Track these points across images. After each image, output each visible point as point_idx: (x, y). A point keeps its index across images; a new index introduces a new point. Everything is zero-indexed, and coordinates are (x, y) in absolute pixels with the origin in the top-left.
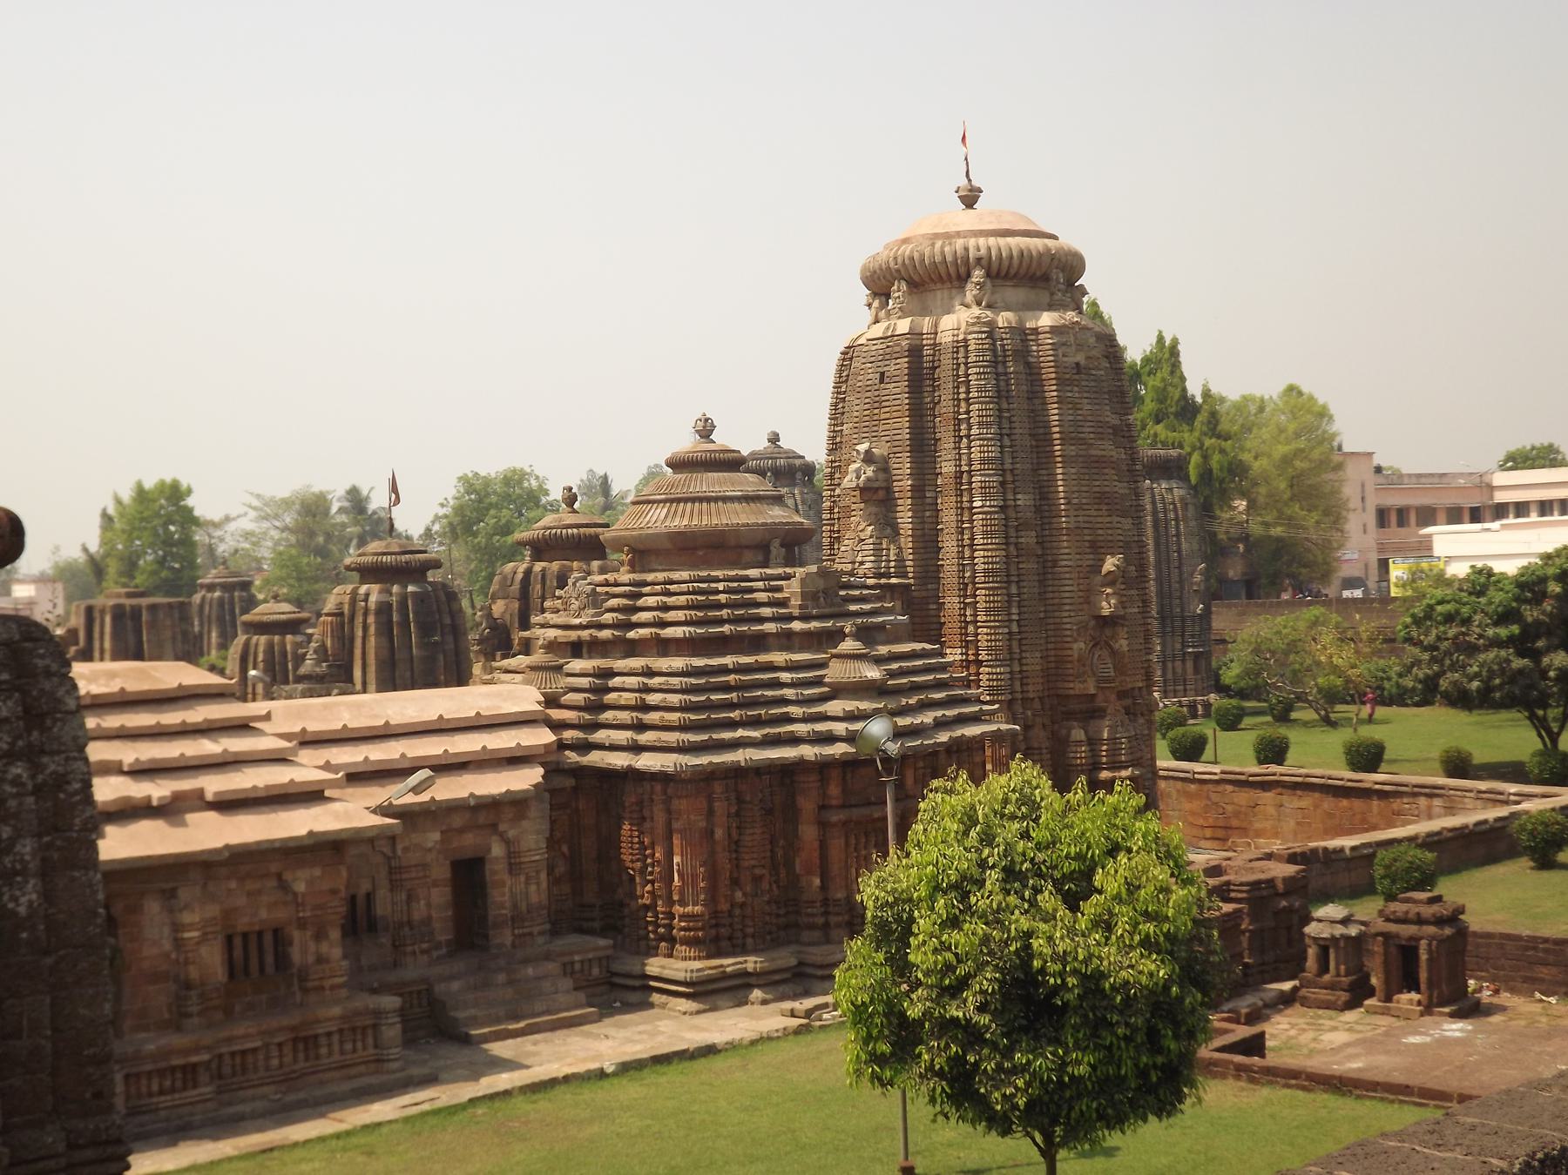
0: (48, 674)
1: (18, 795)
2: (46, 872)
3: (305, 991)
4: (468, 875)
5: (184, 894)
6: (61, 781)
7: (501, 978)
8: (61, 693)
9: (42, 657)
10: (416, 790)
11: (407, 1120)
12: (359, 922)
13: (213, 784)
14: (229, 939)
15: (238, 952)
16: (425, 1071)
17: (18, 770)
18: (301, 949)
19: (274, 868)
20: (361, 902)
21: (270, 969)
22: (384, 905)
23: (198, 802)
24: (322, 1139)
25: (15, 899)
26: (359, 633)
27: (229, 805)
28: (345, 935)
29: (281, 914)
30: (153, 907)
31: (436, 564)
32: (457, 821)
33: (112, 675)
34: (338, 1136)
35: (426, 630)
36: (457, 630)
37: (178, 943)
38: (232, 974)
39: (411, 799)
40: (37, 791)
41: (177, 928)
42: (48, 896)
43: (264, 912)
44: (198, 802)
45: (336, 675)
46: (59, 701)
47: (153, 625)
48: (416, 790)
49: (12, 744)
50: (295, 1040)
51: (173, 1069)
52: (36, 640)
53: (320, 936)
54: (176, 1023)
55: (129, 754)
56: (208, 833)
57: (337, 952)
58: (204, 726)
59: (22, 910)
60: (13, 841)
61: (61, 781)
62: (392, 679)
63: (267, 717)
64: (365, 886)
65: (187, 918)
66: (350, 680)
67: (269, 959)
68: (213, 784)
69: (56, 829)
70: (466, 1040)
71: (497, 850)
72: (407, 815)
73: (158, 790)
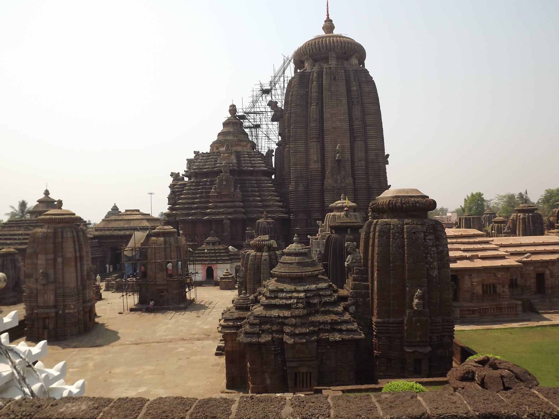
0: (440, 231)
3: (500, 298)
4: (540, 277)
5: (473, 275)
6: (442, 251)
7: (548, 300)
10: (526, 258)
11: (521, 328)
12: (513, 284)
13: (480, 254)
14: (483, 285)
15: (485, 288)
16: (527, 318)
18: (499, 289)
19: (493, 272)
20: (514, 281)
21: (492, 293)
22: (519, 281)
23: (477, 257)
24: (500, 329)
26: (518, 224)
27: (484, 258)
28: (509, 286)
29: (495, 281)
30: (467, 278)
31: (537, 209)
32: (538, 265)
33: (459, 231)
34: (504, 329)
35: (534, 223)
36: (542, 223)
37: (472, 285)
38: (483, 292)
39: (525, 259)
40: (438, 253)
41: (472, 282)
42: (439, 273)
43: (491, 281)
44: (477, 257)
45: (513, 232)
47: (473, 221)
48: (526, 258)
50: (497, 308)
51: (470, 310)
53: (503, 287)
54: (471, 301)
55: (463, 247)
56: (479, 264)
57: (507, 290)
60: (432, 263)
61: (442, 251)
62: (525, 234)
63: (493, 241)
64: (515, 277)
65: (474, 280)
66: (516, 234)
67: (492, 290)
68: (480, 254)
70: (538, 313)
71: (548, 272)
72: (524, 263)
73: (468, 254)
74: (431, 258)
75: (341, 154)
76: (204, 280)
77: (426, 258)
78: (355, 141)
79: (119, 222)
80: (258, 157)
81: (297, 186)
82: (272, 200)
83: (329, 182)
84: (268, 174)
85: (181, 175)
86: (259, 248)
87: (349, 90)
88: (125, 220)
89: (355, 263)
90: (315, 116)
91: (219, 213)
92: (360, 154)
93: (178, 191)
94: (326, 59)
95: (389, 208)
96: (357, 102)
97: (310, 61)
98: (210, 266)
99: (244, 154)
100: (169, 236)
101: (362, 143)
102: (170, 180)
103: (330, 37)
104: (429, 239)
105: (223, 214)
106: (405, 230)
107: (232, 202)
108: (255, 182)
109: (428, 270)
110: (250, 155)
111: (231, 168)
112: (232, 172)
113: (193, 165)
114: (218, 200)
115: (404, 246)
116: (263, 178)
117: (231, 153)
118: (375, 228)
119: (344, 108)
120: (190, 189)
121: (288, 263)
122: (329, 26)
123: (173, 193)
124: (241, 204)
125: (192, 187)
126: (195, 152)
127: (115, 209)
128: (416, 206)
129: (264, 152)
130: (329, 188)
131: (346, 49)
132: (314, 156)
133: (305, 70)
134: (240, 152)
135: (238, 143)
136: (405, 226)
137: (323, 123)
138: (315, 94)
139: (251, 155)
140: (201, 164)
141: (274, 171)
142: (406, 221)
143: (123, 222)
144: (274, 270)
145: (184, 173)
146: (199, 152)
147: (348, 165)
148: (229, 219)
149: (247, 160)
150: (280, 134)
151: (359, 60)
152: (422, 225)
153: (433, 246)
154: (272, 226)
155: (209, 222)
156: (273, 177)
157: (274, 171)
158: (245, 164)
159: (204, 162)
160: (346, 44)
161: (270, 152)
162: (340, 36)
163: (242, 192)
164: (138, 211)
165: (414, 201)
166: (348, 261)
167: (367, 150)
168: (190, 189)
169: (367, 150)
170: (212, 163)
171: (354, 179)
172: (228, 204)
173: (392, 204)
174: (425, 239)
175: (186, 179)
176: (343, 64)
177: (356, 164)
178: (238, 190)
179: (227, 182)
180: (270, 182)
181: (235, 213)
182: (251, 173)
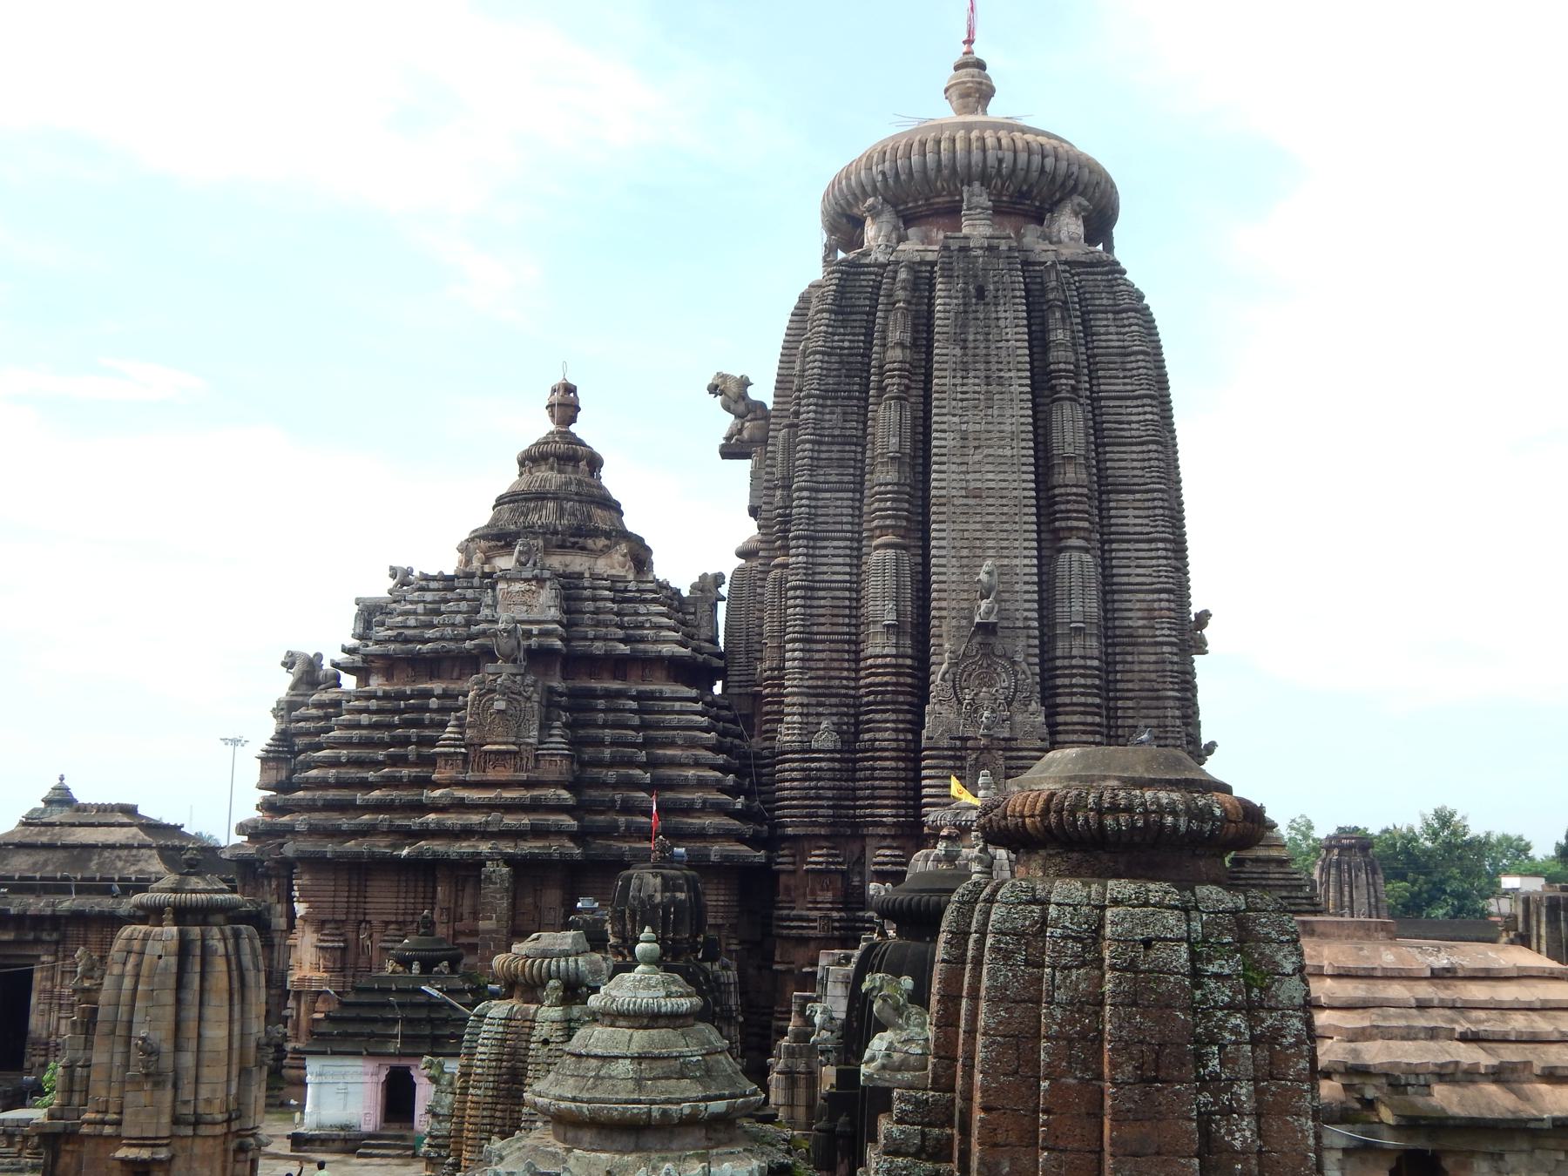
0: (1270, 941)
1: (1236, 1043)
2: (1258, 1115)
8: (1279, 957)
9: (1264, 925)
17: (1237, 1020)
25: (1231, 1133)
40: (1255, 1041)
42: (1260, 1133)
46: (1277, 964)
49: (1232, 999)
52: (1256, 910)
58: (1538, 1005)
59: (1238, 1144)
60: (1231, 1081)
69: (1273, 1078)
74: (1221, 1063)
75: (996, 600)
76: (368, 1127)
77: (1200, 1059)
78: (1061, 550)
79: (41, 856)
80: (654, 601)
81: (808, 730)
82: (702, 784)
83: (939, 718)
84: (694, 672)
85: (326, 665)
86: (526, 987)
87: (1039, 342)
88: (65, 847)
89: (899, 1069)
90: (894, 440)
91: (466, 833)
92: (1079, 606)
93: (307, 733)
94: (952, 213)
95: (1048, 829)
96: (1074, 389)
97: (888, 216)
98: (404, 1062)
99: (595, 589)
100: (205, 923)
101: (1087, 557)
102: (282, 684)
103: (968, 127)
104: (1217, 976)
105: (485, 835)
106: (1108, 930)
107: (528, 785)
108: (633, 705)
109: (1205, 1119)
110: (621, 595)
111: (534, 642)
112: (539, 658)
113: (383, 624)
114: (471, 776)
115: (1101, 1004)
116: (669, 689)
117: (540, 581)
118: (987, 914)
119: (1016, 414)
120: (358, 726)
121: (596, 1057)
122: (974, 85)
123: (283, 737)
124: (565, 794)
125: (364, 719)
126: (394, 573)
127: (61, 798)
128: (1162, 826)
129: (683, 582)
130: (945, 743)
131: (1035, 174)
132: (881, 607)
133: (867, 254)
134: (580, 576)
135: (577, 537)
136: (1108, 913)
137: (927, 473)
138: (897, 353)
139: (626, 590)
140: (412, 621)
141: (721, 663)
142: (1115, 887)
143: (61, 854)
144: (538, 1086)
145: (341, 657)
146: (409, 572)
147: (1023, 649)
148: (509, 860)
149: (611, 611)
150: (753, 512)
151: (1086, 221)
152: (1186, 910)
153: (1232, 1007)
154: (681, 896)
155: (425, 870)
156: (718, 688)
157: (721, 663)
158: (598, 624)
159: (427, 612)
160: (1036, 159)
161: (708, 586)
162: (1011, 128)
163: (575, 743)
164: (130, 810)
165: (1157, 801)
166: (873, 1059)
167: (1108, 588)
168: (358, 726)
169: (1108, 588)
170: (459, 618)
171: (1052, 711)
172: (507, 794)
173: (1059, 812)
174: (1196, 975)
175: (349, 682)
176: (1019, 236)
177: (1061, 647)
178: (558, 739)
179: (509, 701)
180: (699, 706)
181: (537, 832)
182: (618, 666)
